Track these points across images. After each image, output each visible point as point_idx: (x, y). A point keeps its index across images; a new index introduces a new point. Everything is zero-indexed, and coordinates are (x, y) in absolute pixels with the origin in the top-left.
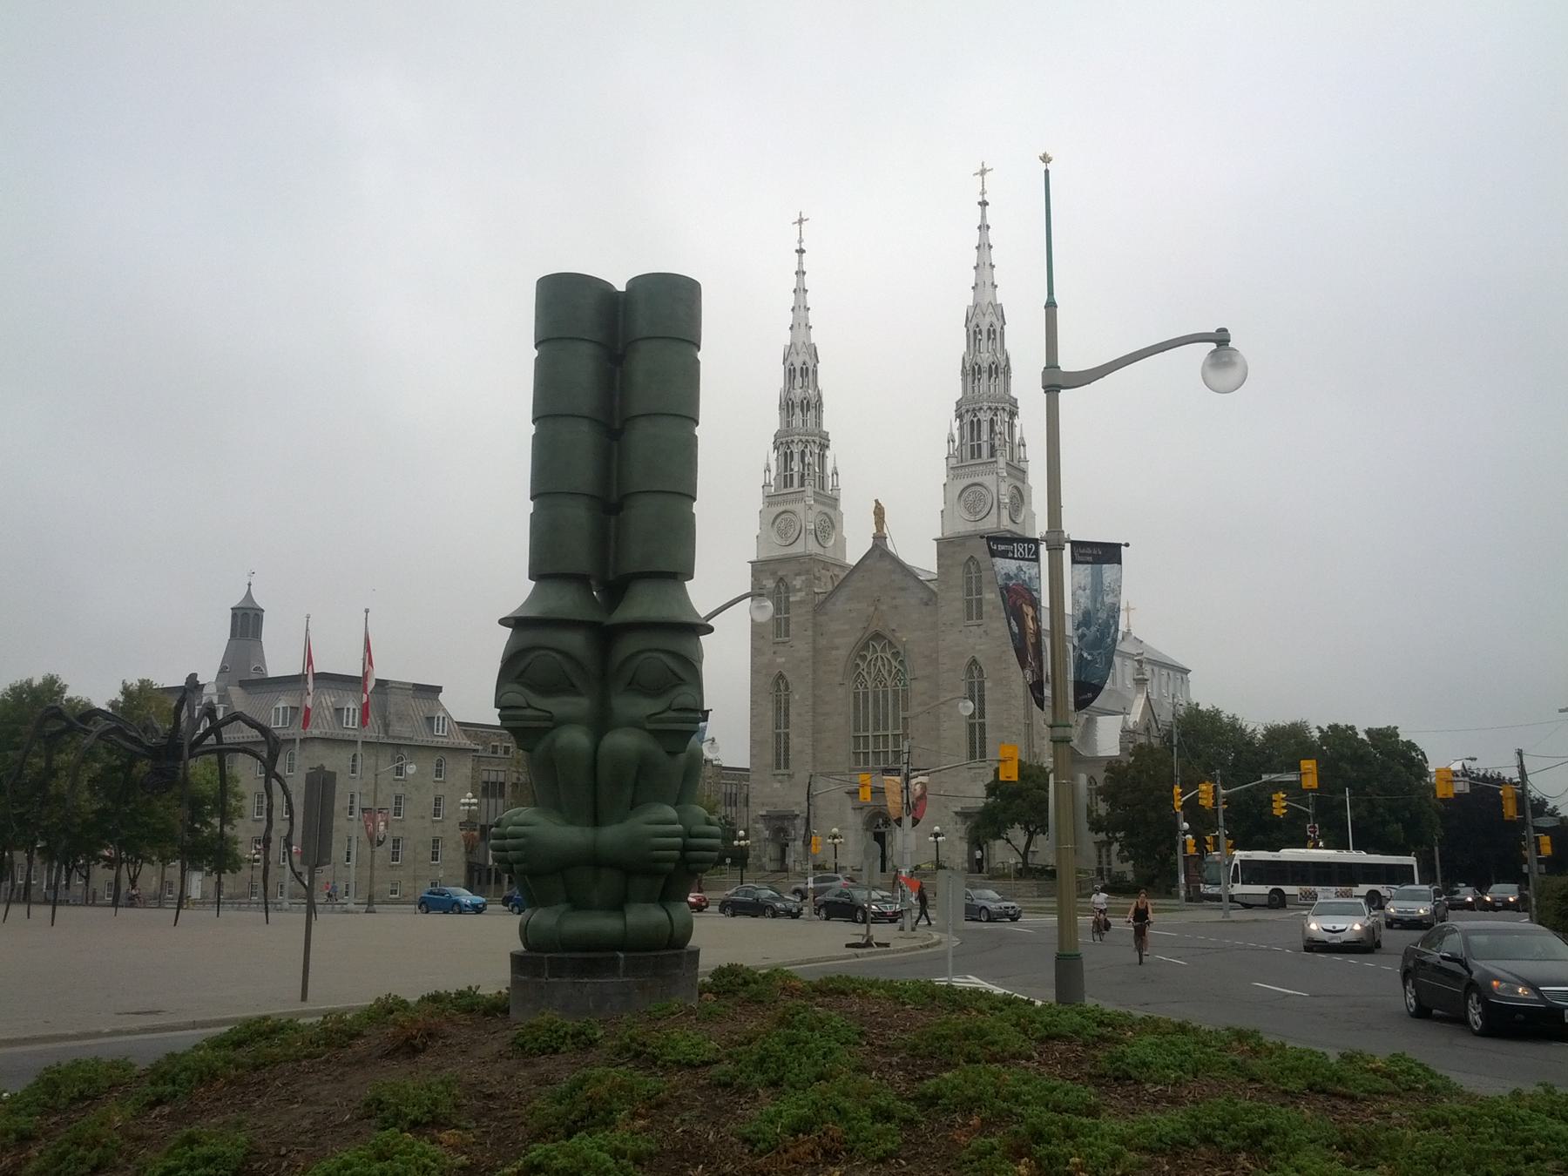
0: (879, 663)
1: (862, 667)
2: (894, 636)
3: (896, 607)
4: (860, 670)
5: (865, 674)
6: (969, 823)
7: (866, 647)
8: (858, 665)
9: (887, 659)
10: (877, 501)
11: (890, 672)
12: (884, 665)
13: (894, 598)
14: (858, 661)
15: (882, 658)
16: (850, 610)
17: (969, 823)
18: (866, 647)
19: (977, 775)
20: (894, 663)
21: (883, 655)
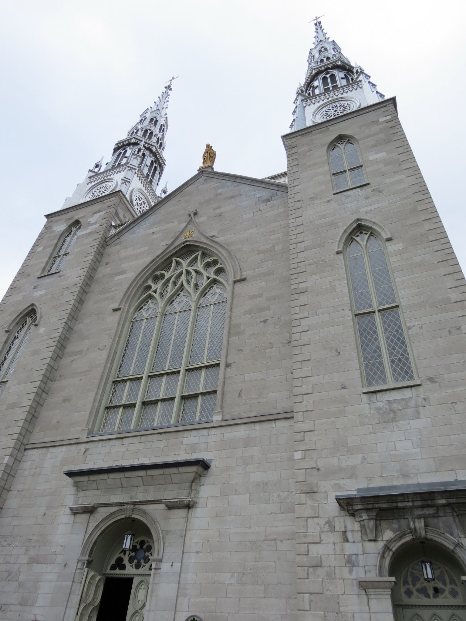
0: (183, 278)
1: (153, 288)
2: (212, 241)
3: (221, 215)
4: (151, 292)
5: (157, 296)
6: (388, 535)
7: (166, 264)
8: (149, 287)
9: (197, 272)
10: (208, 146)
11: (196, 286)
12: (188, 282)
13: (219, 207)
14: (150, 283)
15: (188, 272)
16: (153, 233)
17: (388, 535)
18: (166, 264)
19: (395, 406)
20: (205, 274)
21: (190, 269)
